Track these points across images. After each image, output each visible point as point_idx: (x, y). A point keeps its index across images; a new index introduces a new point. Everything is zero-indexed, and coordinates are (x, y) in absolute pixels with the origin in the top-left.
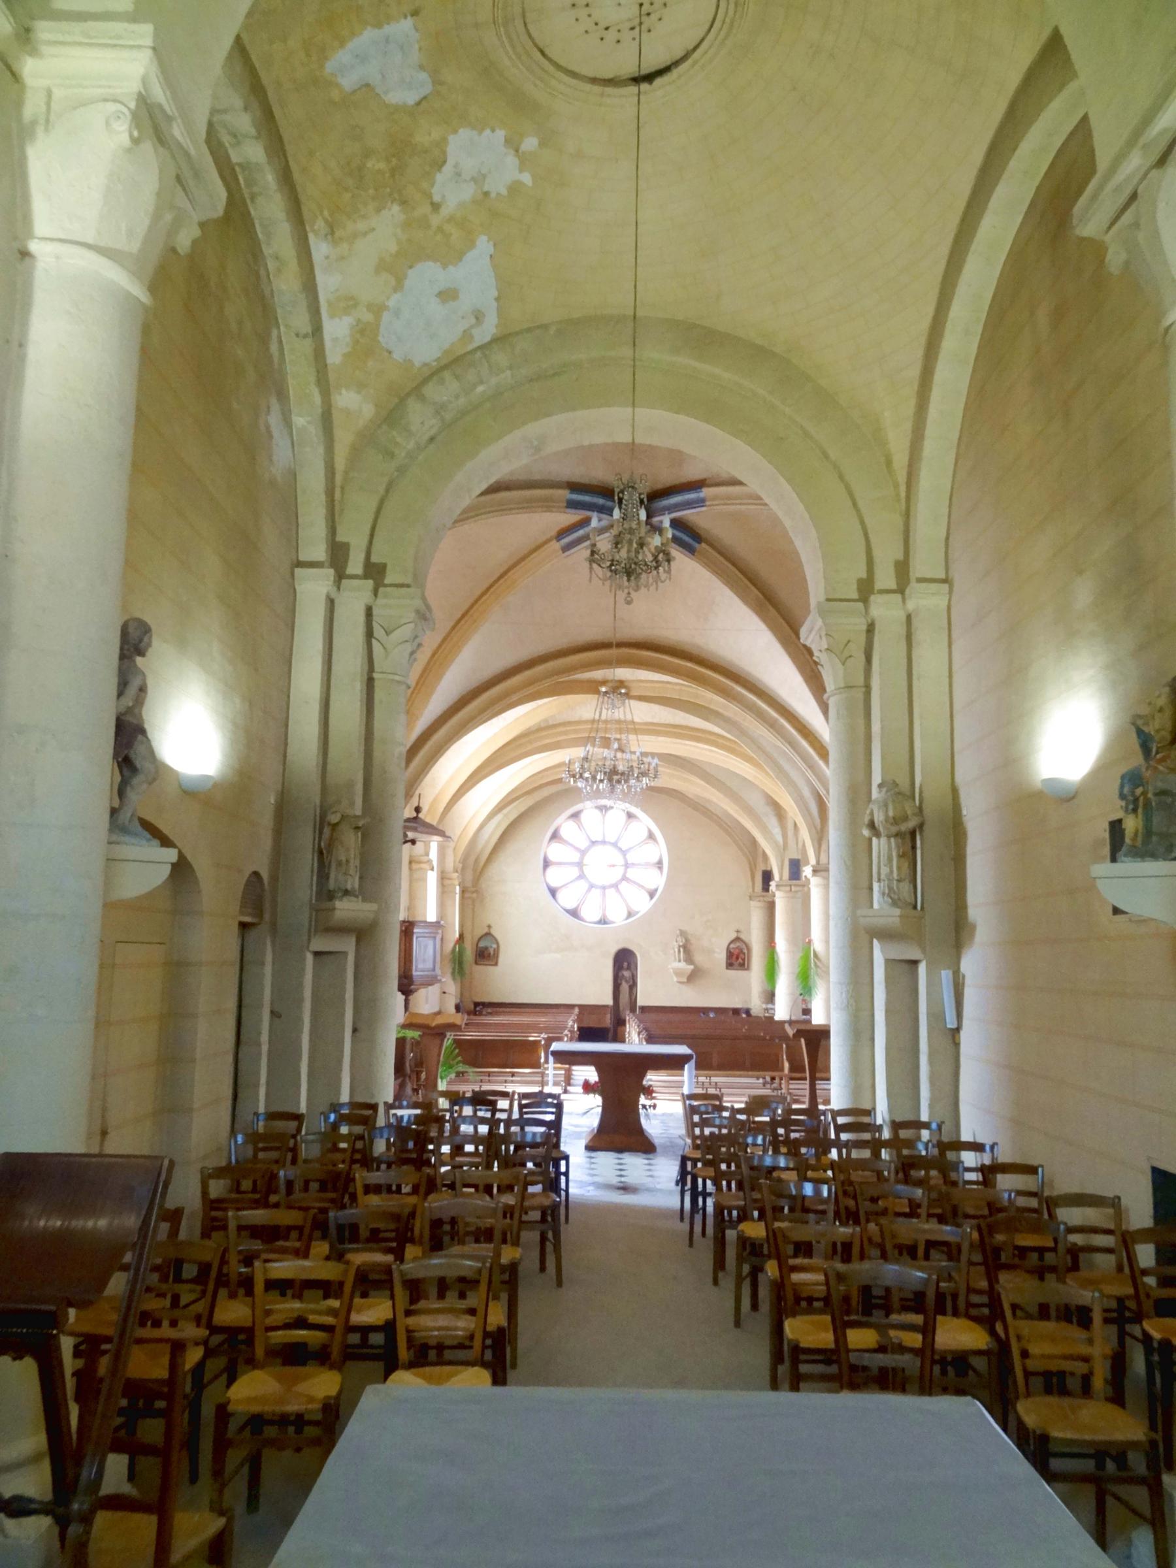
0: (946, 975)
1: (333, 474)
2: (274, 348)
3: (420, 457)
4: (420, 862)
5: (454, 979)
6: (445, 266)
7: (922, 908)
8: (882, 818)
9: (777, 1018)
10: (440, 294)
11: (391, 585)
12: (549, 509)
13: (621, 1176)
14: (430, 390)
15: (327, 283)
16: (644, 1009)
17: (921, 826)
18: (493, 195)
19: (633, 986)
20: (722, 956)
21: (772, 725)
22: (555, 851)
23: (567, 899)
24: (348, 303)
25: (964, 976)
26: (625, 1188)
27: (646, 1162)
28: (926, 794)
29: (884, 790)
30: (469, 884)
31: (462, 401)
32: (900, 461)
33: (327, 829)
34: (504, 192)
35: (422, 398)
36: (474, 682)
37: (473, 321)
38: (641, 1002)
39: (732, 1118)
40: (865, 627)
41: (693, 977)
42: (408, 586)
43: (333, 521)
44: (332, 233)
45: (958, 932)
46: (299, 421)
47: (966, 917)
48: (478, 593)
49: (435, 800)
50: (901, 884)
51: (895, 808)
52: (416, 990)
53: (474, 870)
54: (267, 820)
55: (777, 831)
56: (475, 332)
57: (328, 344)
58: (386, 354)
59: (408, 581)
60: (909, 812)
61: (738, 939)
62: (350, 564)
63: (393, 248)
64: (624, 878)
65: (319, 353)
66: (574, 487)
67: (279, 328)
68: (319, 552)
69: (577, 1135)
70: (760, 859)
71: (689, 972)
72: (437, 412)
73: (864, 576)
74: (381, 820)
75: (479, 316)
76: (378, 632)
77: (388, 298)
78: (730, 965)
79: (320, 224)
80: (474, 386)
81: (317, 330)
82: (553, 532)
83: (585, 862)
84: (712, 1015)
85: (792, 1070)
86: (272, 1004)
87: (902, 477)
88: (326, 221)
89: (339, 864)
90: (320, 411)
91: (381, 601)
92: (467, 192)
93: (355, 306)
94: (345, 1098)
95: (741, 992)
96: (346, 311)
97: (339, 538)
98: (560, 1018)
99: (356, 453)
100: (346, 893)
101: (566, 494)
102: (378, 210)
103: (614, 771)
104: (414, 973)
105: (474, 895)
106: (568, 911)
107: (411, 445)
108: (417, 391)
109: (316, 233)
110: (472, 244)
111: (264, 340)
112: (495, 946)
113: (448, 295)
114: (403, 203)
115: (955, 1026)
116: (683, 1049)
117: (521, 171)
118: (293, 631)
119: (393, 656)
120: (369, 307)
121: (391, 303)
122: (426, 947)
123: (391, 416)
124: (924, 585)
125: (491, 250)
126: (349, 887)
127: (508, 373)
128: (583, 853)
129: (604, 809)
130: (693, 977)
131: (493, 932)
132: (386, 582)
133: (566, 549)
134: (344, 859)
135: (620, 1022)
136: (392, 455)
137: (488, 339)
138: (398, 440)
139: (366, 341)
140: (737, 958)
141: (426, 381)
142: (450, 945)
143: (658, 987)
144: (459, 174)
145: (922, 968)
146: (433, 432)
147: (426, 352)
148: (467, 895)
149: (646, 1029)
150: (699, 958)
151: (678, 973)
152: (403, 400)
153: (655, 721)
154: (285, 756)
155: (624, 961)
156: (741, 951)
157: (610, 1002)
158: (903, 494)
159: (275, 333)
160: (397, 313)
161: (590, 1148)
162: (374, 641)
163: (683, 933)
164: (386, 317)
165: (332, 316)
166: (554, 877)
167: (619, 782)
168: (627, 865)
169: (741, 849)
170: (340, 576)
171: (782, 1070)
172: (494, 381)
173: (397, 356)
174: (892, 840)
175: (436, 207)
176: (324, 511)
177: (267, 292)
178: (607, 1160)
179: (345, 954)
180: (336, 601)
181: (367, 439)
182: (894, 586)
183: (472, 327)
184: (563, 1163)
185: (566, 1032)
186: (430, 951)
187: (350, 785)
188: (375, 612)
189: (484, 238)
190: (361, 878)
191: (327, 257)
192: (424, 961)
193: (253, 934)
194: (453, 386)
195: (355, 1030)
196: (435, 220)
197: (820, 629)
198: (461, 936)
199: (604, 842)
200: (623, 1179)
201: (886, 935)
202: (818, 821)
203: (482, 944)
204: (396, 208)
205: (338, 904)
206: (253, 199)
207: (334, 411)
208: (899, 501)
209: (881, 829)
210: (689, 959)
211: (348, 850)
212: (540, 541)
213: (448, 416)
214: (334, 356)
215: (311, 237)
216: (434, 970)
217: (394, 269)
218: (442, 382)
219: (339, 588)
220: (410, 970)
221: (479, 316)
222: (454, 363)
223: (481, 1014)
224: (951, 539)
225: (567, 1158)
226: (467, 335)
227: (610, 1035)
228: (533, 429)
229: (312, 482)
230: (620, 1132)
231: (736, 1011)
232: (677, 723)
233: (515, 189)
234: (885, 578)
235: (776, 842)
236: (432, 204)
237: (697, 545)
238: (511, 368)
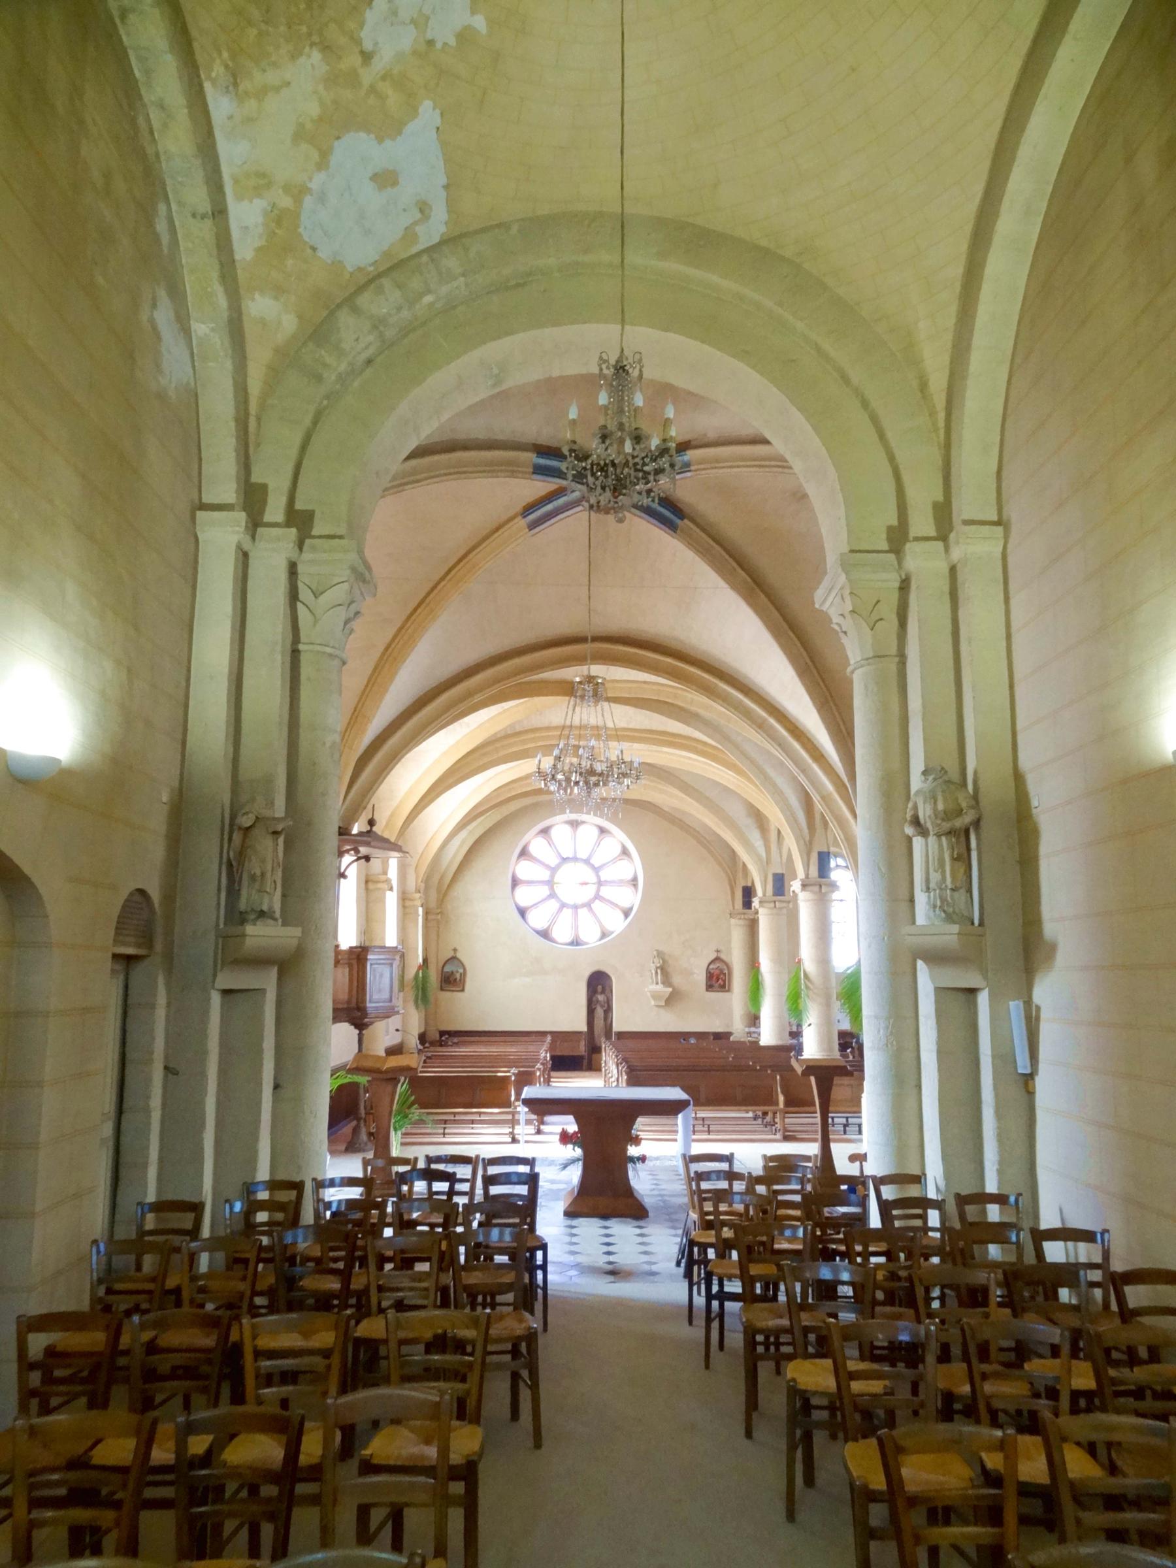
0: (1015, 1007)
1: (246, 402)
2: (161, 226)
3: (356, 384)
4: (378, 882)
5: (417, 1007)
6: (380, 140)
7: (981, 924)
8: (929, 812)
9: (762, 1043)
10: (375, 178)
11: (320, 537)
12: (513, 474)
13: (609, 1253)
14: (363, 300)
15: (232, 153)
16: (621, 1035)
17: (977, 823)
18: (439, 45)
19: (608, 1010)
20: (701, 977)
21: (760, 726)
22: (524, 869)
23: (537, 919)
24: (261, 182)
25: (1038, 1008)
26: (614, 1273)
27: (638, 1231)
28: (981, 784)
29: (931, 778)
30: (433, 904)
31: (405, 314)
32: (938, 383)
33: (239, 833)
34: (452, 42)
35: (356, 310)
36: (433, 683)
37: (418, 216)
38: (617, 1027)
39: (750, 1190)
40: (897, 585)
41: (672, 1000)
42: (340, 537)
43: (247, 456)
44: (236, 84)
45: (1029, 952)
46: (200, 329)
47: (1039, 933)
48: (437, 578)
49: (392, 815)
50: (956, 894)
51: (945, 800)
52: (372, 1023)
53: (439, 890)
54: (158, 823)
55: (759, 844)
56: (419, 229)
57: (235, 233)
58: (309, 251)
59: (341, 531)
60: (964, 805)
61: (717, 959)
62: (268, 510)
63: (314, 109)
64: (597, 897)
65: (223, 244)
66: (543, 451)
67: (169, 205)
68: (225, 490)
69: (554, 1195)
70: (740, 875)
72: (375, 327)
73: (895, 522)
74: (309, 824)
75: (424, 208)
76: (304, 594)
77: (311, 179)
78: (709, 987)
79: (218, 70)
80: (421, 295)
81: (219, 212)
82: (519, 508)
83: (556, 880)
84: (693, 1041)
85: (788, 1103)
86: (166, 1057)
87: (940, 401)
88: (227, 66)
89: (253, 878)
90: (226, 315)
91: (307, 556)
92: (407, 39)
93: (269, 185)
94: (263, 1173)
95: (725, 1015)
96: (258, 191)
97: (256, 478)
98: (532, 1048)
99: (275, 375)
100: (262, 914)
101: (532, 457)
102: (294, 56)
103: (592, 772)
104: (368, 1005)
106: (538, 932)
107: (343, 367)
108: (349, 302)
109: (214, 82)
110: (413, 112)
111: (147, 212)
112: (461, 971)
113: (386, 179)
114: (326, 48)
115: (1028, 1071)
116: (674, 1093)
117: (473, 13)
118: (194, 587)
119: (322, 621)
120: (287, 188)
121: (314, 185)
122: (381, 975)
123: (318, 333)
124: (973, 528)
125: (438, 121)
126: (265, 908)
127: (462, 279)
128: (554, 870)
129: (575, 824)
131: (459, 955)
132: (315, 532)
133: (533, 526)
134: (258, 873)
135: (595, 1050)
136: (319, 378)
137: (436, 239)
138: (328, 360)
139: (283, 231)
140: (717, 979)
141: (361, 289)
142: (411, 972)
143: (635, 1011)
144: (395, 13)
145: (983, 999)
146: (371, 351)
147: (361, 254)
149: (625, 1060)
150: (677, 980)
151: (655, 996)
152: (332, 313)
153: (631, 726)
154: (184, 743)
155: (598, 983)
156: (722, 972)
157: (584, 1028)
158: (941, 424)
159: (162, 208)
160: (322, 199)
161: (570, 1214)
162: (299, 605)
163: (660, 954)
164: (308, 201)
165: (239, 198)
166: (524, 896)
167: (596, 785)
168: (600, 883)
169: (720, 864)
170: (255, 523)
171: (777, 1104)
172: (444, 289)
173: (324, 253)
174: (943, 838)
175: (367, 57)
176: (234, 440)
177: (150, 151)
178: (590, 1227)
179: (263, 991)
180: (251, 555)
181: (287, 359)
182: (933, 533)
183: (416, 223)
184: (539, 1254)
185: (539, 1066)
186: (386, 980)
187: (269, 780)
188: (301, 569)
189: (427, 104)
190: (284, 896)
191: (230, 118)
192: (380, 991)
193: (139, 973)
194: (395, 296)
195: (276, 1087)
196: (367, 76)
197: (842, 588)
198: (425, 960)
199: (575, 859)
200: (611, 1258)
201: (937, 958)
202: (806, 831)
203: (448, 969)
204: (316, 56)
205: (250, 929)
206: (123, 17)
207: (245, 318)
208: (936, 430)
209: (929, 825)
210: (667, 981)
211: (263, 861)
212: (504, 518)
213: (390, 333)
214: (244, 251)
215: (207, 86)
216: (391, 1001)
217: (319, 136)
218: (380, 291)
219: (253, 537)
220: (364, 1001)
221: (424, 208)
222: (394, 268)
223: (446, 1045)
224: (1005, 473)
225: (544, 1247)
226: (409, 235)
227: (585, 1062)
228: (494, 350)
229: (218, 407)
230: (606, 1192)
231: (718, 1036)
232: (654, 728)
233: (465, 36)
234: (922, 523)
236: (362, 53)
237: (678, 521)
238: (463, 275)
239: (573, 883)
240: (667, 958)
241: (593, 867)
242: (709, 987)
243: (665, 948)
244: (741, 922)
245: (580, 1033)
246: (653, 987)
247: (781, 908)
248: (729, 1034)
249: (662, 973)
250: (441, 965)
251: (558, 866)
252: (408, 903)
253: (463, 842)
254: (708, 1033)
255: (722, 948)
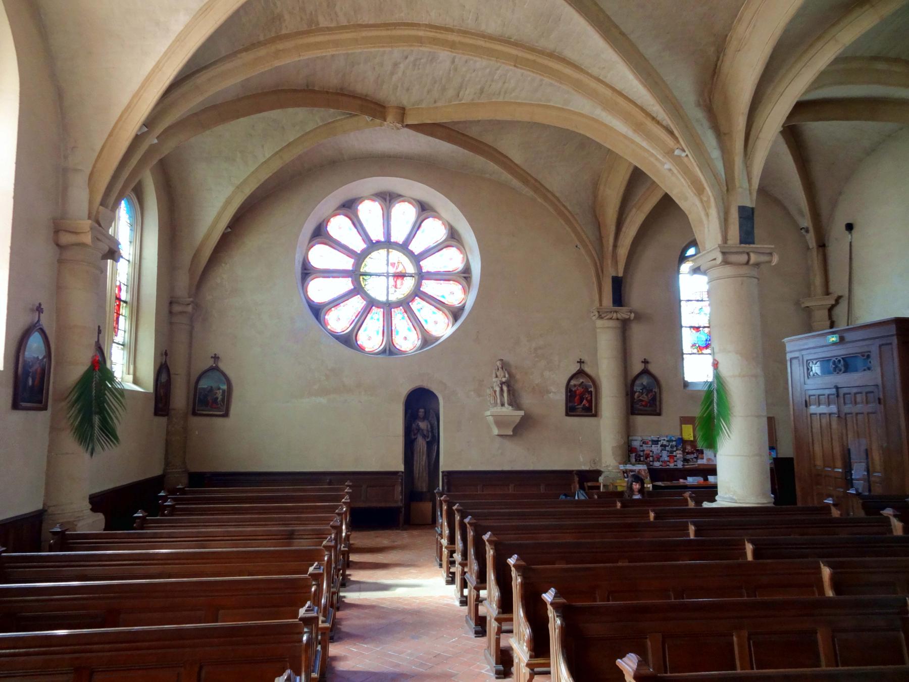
9: (722, 501)
19: (433, 441)
20: (559, 397)
23: (339, 320)
41: (522, 428)
53: (191, 271)
55: (715, 154)
61: (581, 373)
64: (417, 293)
71: (518, 420)
78: (570, 411)
95: (599, 446)
105: (190, 309)
112: (225, 387)
128: (359, 258)
130: (522, 428)
131: (221, 366)
140: (581, 399)
143: (471, 443)
148: (177, 308)
150: (527, 400)
155: (420, 406)
156: (586, 390)
157: (401, 468)
163: (505, 366)
166: (320, 290)
203: (204, 384)
210: (515, 403)
227: (402, 518)
235: (716, 176)
239: (383, 276)
240: (514, 371)
241: (410, 254)
242: (570, 411)
243: (509, 358)
244: (611, 323)
245: (395, 473)
246: (499, 410)
247: (757, 265)
248: (598, 473)
249: (509, 391)
250: (193, 379)
251: (365, 254)
252: (65, 239)
253: (228, 202)
254: (572, 471)
255: (585, 358)
